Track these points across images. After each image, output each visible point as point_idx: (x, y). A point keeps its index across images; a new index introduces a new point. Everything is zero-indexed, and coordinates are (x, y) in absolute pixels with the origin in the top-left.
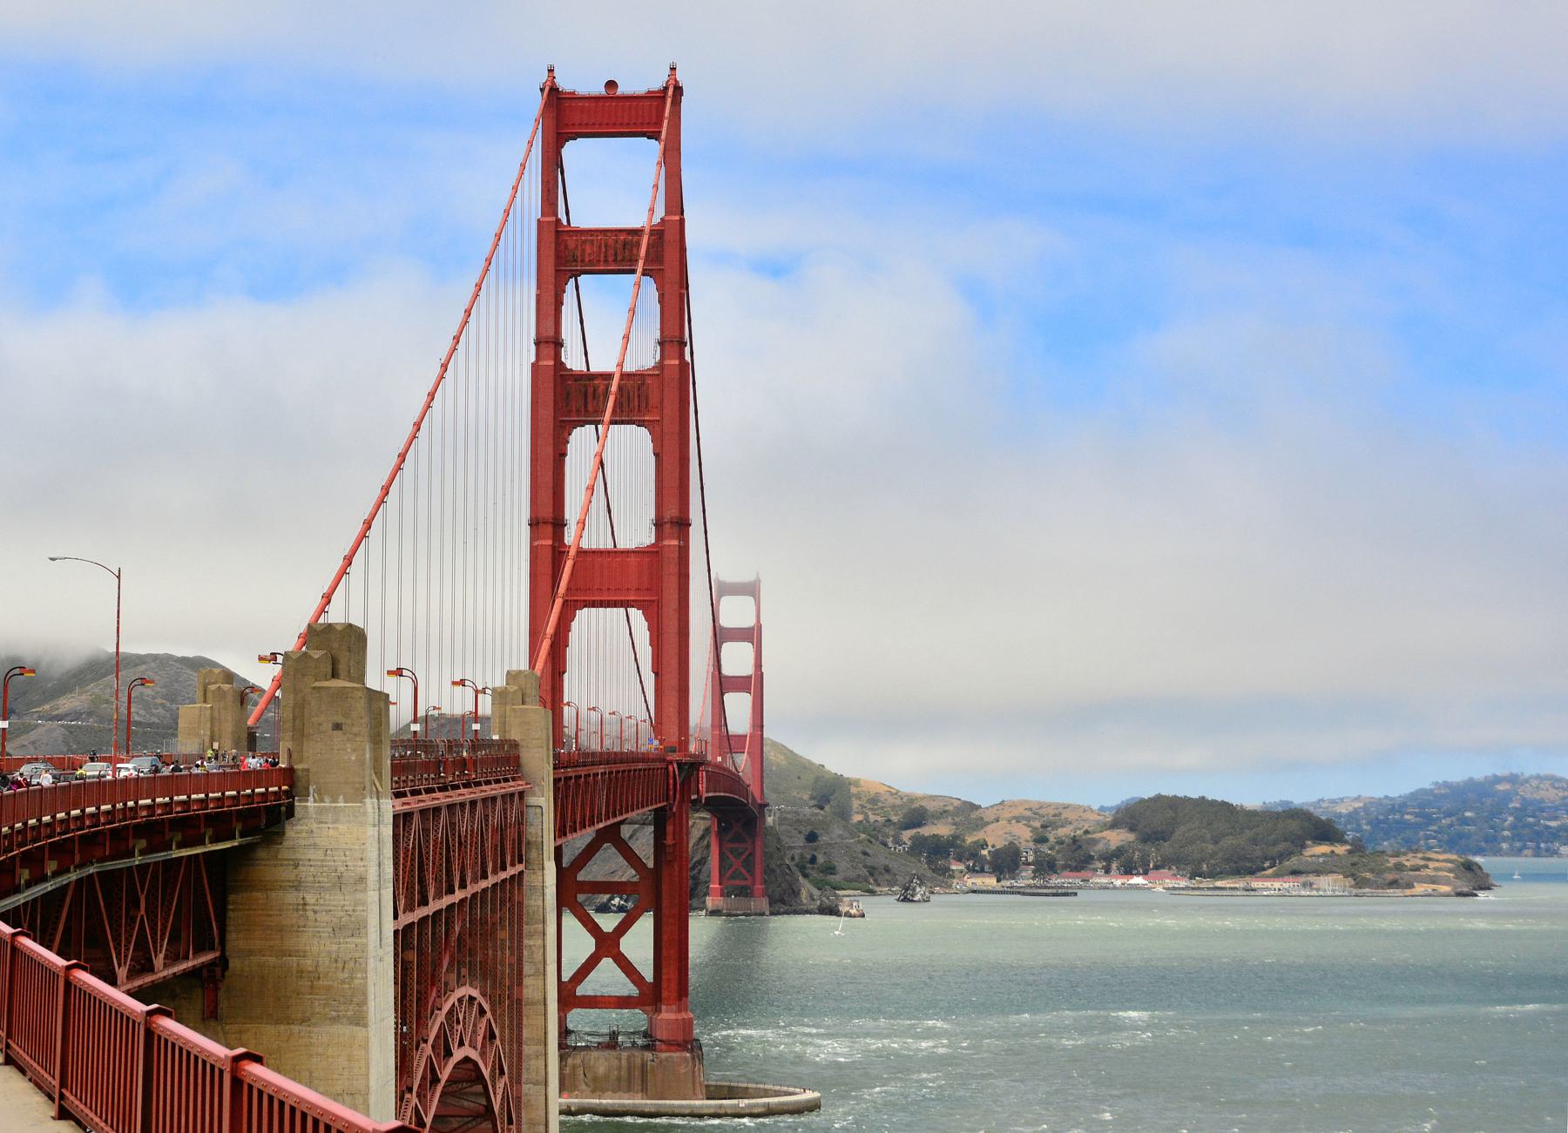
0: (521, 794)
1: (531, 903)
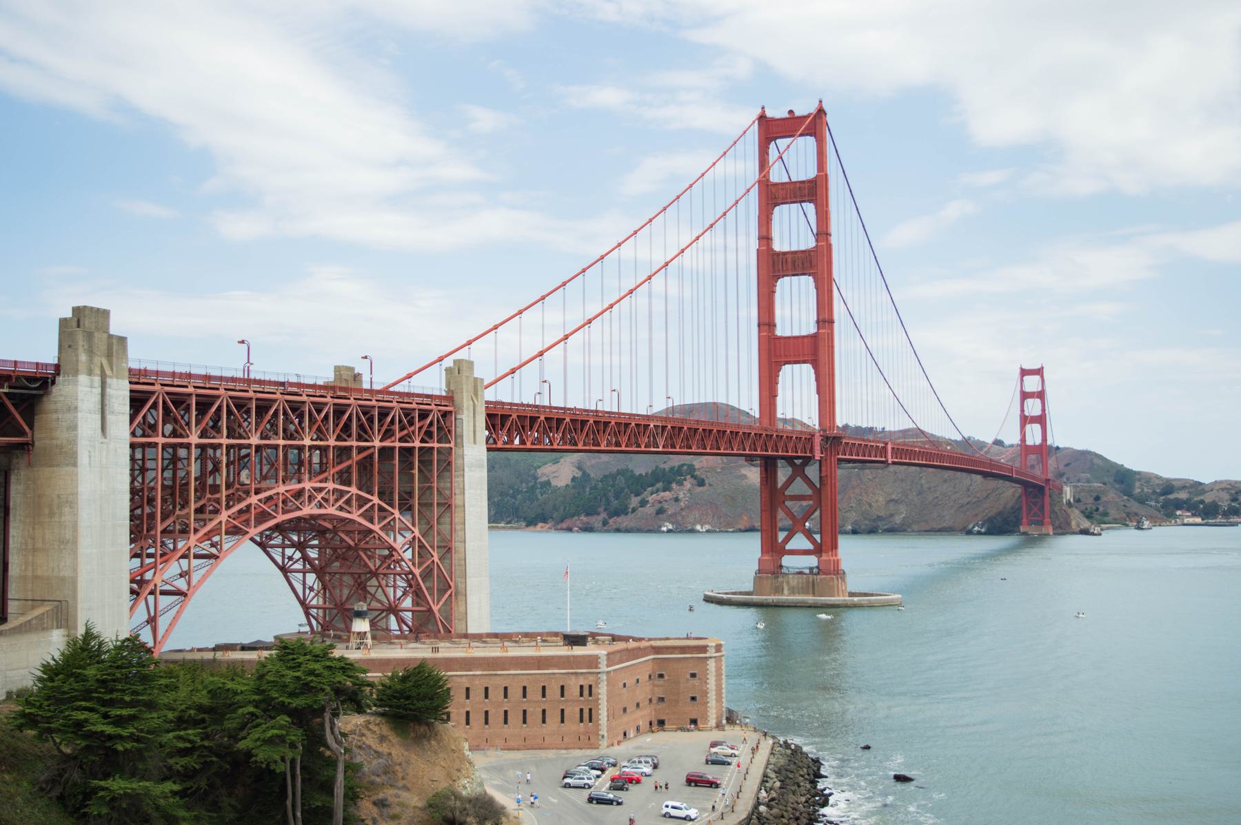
0: (445, 415)
1: (456, 462)
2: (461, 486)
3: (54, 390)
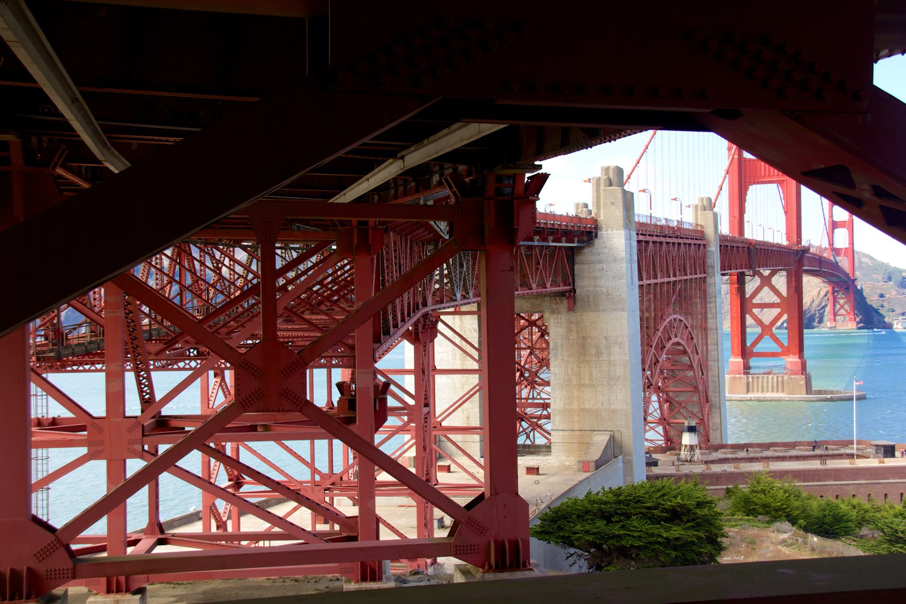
0: (704, 245)
2: (714, 311)
3: (597, 242)
